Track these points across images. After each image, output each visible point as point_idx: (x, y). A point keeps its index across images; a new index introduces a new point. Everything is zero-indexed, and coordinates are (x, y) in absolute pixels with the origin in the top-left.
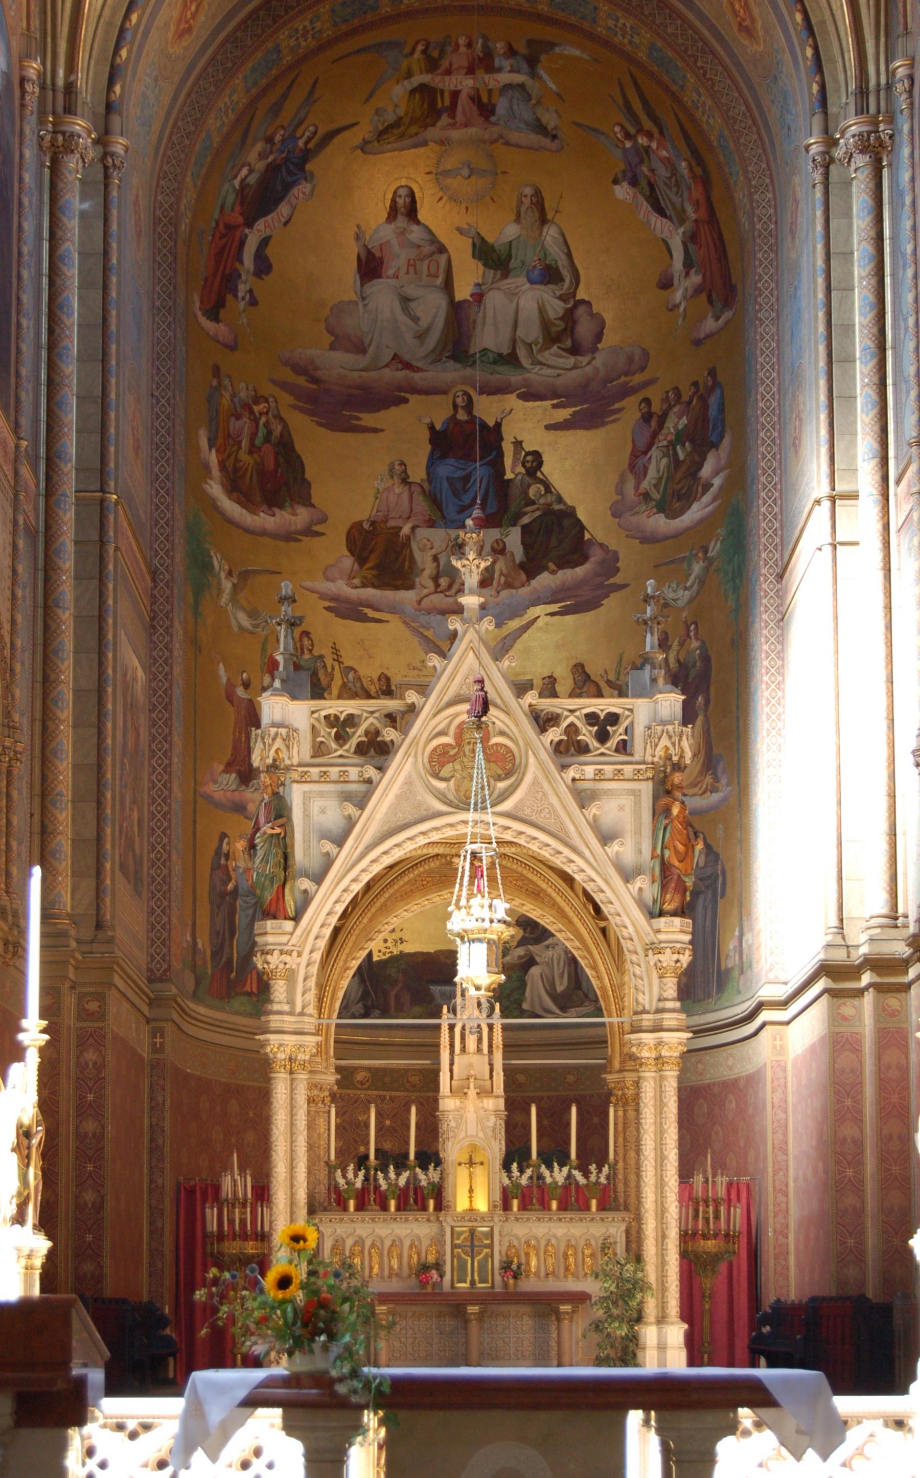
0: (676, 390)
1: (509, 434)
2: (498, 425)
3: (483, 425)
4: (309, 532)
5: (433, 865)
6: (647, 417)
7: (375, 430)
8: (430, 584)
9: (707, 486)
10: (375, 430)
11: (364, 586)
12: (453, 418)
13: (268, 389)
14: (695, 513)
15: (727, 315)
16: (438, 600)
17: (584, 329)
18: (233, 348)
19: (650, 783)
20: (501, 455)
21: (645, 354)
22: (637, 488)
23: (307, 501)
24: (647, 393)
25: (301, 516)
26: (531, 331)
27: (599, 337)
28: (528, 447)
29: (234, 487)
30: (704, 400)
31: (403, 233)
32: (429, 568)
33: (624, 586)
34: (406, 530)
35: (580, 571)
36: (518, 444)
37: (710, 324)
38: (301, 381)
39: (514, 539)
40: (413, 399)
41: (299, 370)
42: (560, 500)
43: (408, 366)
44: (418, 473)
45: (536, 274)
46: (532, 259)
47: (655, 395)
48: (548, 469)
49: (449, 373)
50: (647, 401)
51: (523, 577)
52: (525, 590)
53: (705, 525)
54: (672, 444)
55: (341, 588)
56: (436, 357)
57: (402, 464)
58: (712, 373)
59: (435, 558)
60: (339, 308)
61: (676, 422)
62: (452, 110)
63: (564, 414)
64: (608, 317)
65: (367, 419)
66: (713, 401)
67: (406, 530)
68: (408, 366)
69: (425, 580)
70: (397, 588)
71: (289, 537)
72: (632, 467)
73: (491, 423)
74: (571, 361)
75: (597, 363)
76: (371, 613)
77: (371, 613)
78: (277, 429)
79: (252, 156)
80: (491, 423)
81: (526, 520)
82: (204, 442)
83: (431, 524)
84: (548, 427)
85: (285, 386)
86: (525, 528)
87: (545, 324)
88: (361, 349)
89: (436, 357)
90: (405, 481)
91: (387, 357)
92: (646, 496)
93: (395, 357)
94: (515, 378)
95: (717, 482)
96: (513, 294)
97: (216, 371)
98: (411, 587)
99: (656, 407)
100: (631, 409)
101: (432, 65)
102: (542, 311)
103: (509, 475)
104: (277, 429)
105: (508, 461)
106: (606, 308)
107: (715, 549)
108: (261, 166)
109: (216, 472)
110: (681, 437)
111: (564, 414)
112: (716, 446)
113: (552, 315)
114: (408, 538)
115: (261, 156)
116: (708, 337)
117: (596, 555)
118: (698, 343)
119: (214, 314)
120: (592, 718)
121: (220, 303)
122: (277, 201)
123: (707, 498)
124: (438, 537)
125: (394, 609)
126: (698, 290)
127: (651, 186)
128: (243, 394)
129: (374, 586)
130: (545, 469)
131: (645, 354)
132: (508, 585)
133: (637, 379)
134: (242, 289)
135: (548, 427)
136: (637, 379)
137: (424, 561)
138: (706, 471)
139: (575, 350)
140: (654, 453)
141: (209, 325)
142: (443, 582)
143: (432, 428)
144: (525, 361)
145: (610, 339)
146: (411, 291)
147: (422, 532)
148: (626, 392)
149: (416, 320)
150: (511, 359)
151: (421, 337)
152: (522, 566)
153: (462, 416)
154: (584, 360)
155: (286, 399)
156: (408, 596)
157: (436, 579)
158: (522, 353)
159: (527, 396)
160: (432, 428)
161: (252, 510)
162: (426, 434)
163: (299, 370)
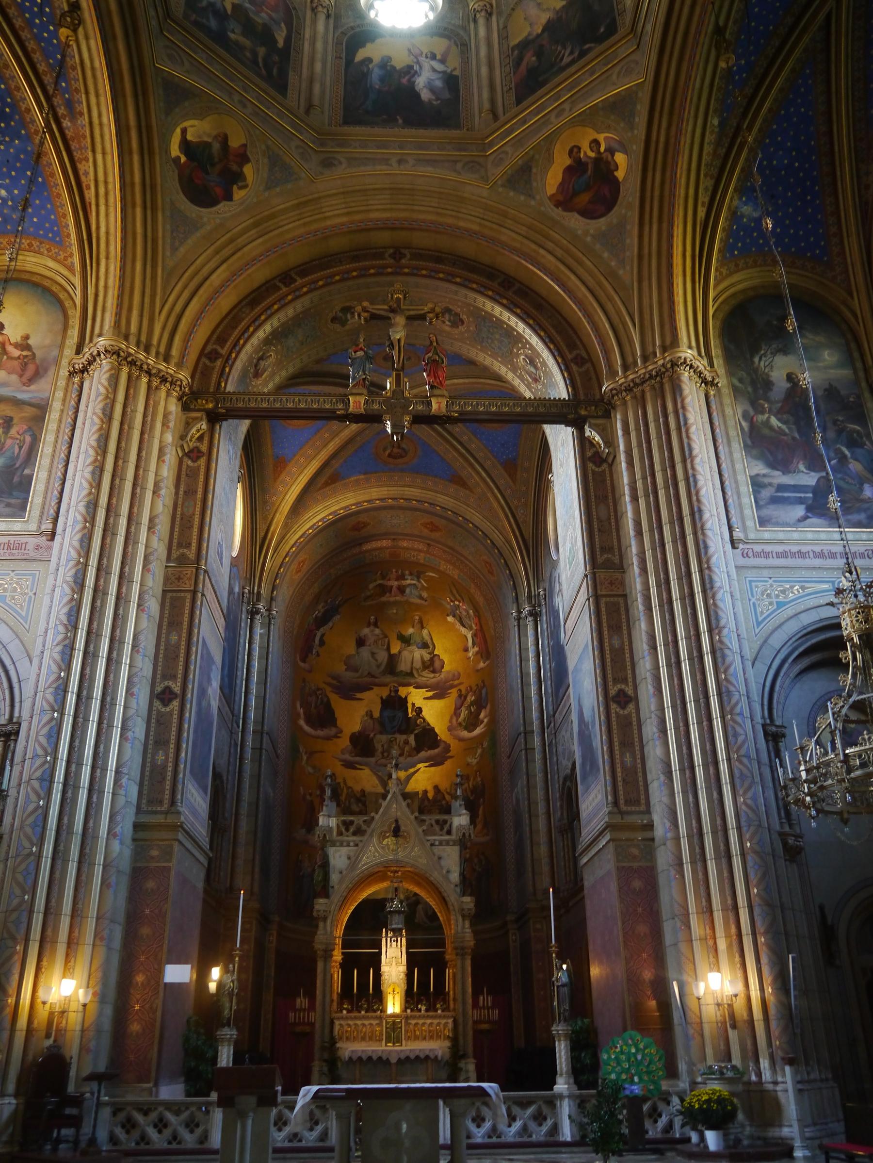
0: (471, 687)
1: (410, 700)
2: (406, 697)
3: (400, 697)
4: (336, 737)
5: (380, 874)
6: (460, 696)
7: (361, 699)
8: (380, 755)
9: (482, 722)
10: (361, 699)
11: (356, 756)
12: (389, 696)
13: (323, 686)
14: (478, 731)
15: (487, 662)
16: (383, 761)
17: (437, 664)
18: (310, 671)
19: (457, 848)
20: (407, 708)
21: (459, 674)
22: (457, 720)
23: (335, 725)
24: (461, 687)
25: (333, 731)
26: (418, 664)
27: (442, 667)
28: (417, 706)
29: (308, 722)
30: (480, 691)
31: (372, 631)
32: (380, 750)
33: (451, 757)
34: (372, 735)
35: (436, 751)
36: (413, 705)
37: (482, 665)
38: (334, 682)
39: (412, 739)
40: (376, 688)
41: (333, 678)
42: (429, 724)
43: (373, 676)
44: (376, 714)
45: (420, 645)
46: (418, 640)
47: (463, 688)
48: (425, 713)
49: (388, 679)
50: (460, 690)
51: (415, 752)
52: (416, 758)
53: (482, 736)
54: (469, 706)
55: (347, 757)
56: (384, 673)
57: (371, 711)
58: (483, 682)
59: (383, 746)
60: (349, 657)
61: (471, 698)
62: (390, 592)
63: (430, 694)
64: (446, 661)
65: (358, 695)
66: (484, 692)
67: (372, 735)
68: (373, 676)
69: (378, 753)
70: (368, 757)
71: (328, 738)
72: (455, 713)
73: (404, 697)
74: (432, 675)
75: (442, 676)
76: (358, 766)
77: (358, 766)
78: (325, 700)
79: (320, 607)
80: (404, 697)
81: (416, 732)
82: (298, 706)
83: (381, 733)
84: (425, 698)
85: (329, 684)
86: (416, 736)
87: (423, 662)
88: (356, 670)
89: (384, 673)
90: (371, 717)
91: (366, 673)
92: (460, 724)
93: (369, 673)
94: (412, 681)
95: (486, 720)
96: (412, 652)
97: (304, 680)
98: (372, 756)
99: (463, 692)
100: (454, 693)
101: (383, 577)
102: (422, 658)
103: (410, 715)
104: (325, 700)
105: (410, 710)
106: (445, 657)
107: (485, 745)
108: (322, 610)
109: (302, 716)
110: (472, 704)
111: (430, 694)
112: (485, 707)
113: (425, 659)
114: (372, 740)
115: (323, 607)
116: (482, 669)
117: (442, 746)
118: (478, 671)
119: (304, 660)
120: (437, 822)
121: (307, 656)
122: (329, 620)
123: (482, 726)
124: (384, 738)
125: (366, 764)
126: (477, 653)
127: (460, 618)
128: (313, 688)
129: (360, 756)
130: (423, 713)
131: (459, 674)
132: (410, 756)
133: (456, 682)
134: (314, 651)
135: (425, 698)
136: (456, 682)
137: (379, 747)
138: (482, 716)
139: (434, 672)
140: (463, 709)
141: (302, 664)
142: (385, 754)
143: (382, 698)
144: (416, 675)
145: (446, 668)
146: (375, 651)
147: (379, 737)
148: (452, 687)
149: (377, 660)
150: (411, 674)
151: (379, 666)
152: (415, 749)
153: (393, 694)
154: (437, 675)
155: (328, 689)
156: (372, 760)
157: (382, 753)
158: (415, 672)
159: (416, 688)
160: (382, 698)
161: (316, 730)
162: (379, 701)
163: (333, 678)
